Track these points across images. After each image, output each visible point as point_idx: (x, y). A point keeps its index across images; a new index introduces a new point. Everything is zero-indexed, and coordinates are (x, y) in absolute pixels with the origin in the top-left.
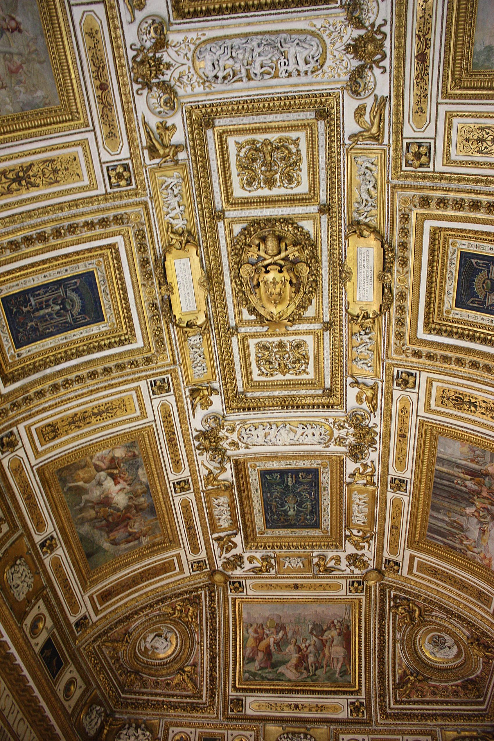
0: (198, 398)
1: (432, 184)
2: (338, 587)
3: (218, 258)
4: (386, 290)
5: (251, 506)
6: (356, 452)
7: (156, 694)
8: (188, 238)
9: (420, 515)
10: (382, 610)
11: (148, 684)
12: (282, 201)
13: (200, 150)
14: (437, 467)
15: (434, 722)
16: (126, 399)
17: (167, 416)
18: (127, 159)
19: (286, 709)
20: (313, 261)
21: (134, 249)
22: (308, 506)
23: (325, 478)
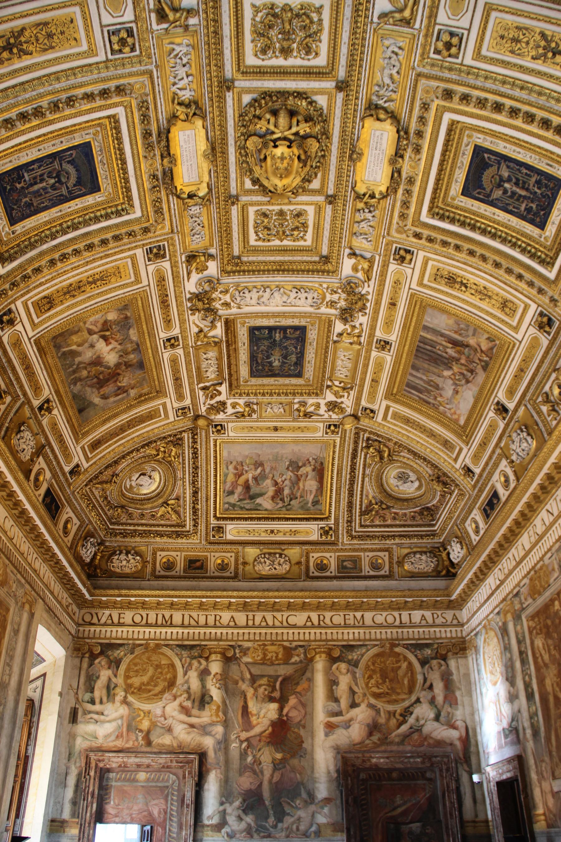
0: (195, 265)
1: (458, 78)
2: (316, 429)
3: (223, 128)
4: (396, 175)
5: (237, 358)
6: (346, 315)
7: (142, 525)
8: (195, 109)
9: (400, 372)
10: (355, 450)
11: (134, 516)
12: (297, 73)
13: (213, 13)
14: (422, 334)
15: (392, 541)
16: (121, 267)
17: (161, 280)
18: (131, 22)
19: (263, 534)
20: (324, 137)
21: (137, 121)
22: (293, 358)
23: (312, 335)
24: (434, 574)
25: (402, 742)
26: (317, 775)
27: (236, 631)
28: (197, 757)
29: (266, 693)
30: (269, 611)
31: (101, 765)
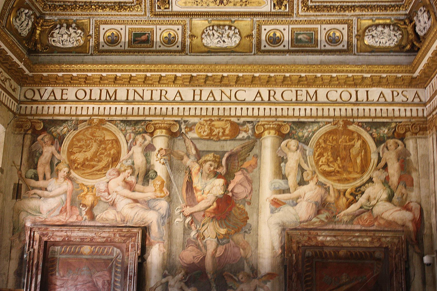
19: (212, 5)
24: (398, 49)
25: (351, 221)
26: (260, 251)
27: (181, 107)
28: (140, 232)
29: (212, 168)
30: (216, 86)
31: (45, 239)
